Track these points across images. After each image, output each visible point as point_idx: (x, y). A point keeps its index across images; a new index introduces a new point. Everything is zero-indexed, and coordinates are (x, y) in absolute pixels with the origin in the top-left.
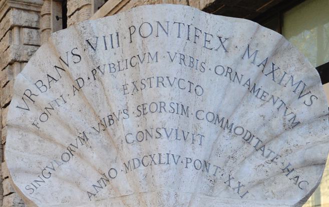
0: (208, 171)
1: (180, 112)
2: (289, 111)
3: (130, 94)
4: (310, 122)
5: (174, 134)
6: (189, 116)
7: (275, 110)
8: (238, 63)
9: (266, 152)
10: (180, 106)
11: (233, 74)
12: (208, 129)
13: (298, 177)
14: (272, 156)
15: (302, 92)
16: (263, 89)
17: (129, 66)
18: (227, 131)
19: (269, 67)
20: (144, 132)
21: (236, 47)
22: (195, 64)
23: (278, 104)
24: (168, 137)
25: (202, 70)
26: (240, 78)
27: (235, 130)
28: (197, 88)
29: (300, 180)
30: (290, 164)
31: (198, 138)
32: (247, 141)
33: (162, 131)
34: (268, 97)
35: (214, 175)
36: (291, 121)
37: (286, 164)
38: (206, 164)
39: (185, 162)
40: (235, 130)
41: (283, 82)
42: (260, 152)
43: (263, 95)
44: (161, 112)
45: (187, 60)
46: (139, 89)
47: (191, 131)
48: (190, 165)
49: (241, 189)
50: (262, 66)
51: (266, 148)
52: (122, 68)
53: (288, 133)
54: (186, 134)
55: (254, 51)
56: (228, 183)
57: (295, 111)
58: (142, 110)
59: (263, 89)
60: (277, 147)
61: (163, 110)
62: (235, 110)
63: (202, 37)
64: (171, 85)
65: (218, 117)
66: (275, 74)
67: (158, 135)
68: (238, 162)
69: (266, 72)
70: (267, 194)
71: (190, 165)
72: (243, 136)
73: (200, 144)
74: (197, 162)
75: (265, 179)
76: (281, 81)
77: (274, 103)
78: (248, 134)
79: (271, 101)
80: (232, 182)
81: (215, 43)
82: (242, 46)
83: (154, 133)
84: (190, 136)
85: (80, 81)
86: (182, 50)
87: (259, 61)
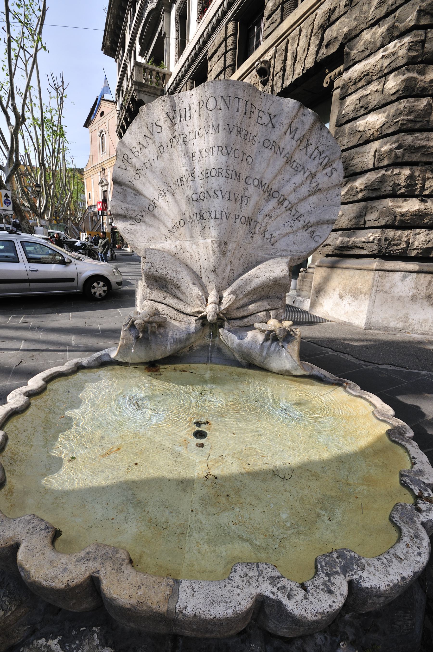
0: (250, 225)
1: (233, 178)
2: (314, 180)
3: (197, 160)
4: (328, 189)
5: (227, 196)
6: (241, 179)
7: (305, 179)
8: (281, 138)
9: (293, 212)
10: (234, 172)
11: (277, 148)
12: (254, 194)
13: (313, 232)
14: (298, 215)
15: (326, 165)
16: (297, 161)
17: (197, 136)
18: (267, 194)
19: (305, 142)
20: (206, 192)
21: (282, 124)
22: (248, 137)
23: (307, 174)
24: (223, 197)
25: (254, 143)
26: (281, 150)
27: (273, 193)
28: (249, 158)
29: (314, 235)
30: (309, 222)
31: (245, 199)
32: (281, 203)
33: (219, 193)
34: (300, 169)
35: (255, 228)
36: (315, 189)
37: (307, 222)
38: (249, 220)
39: (234, 218)
40: (273, 193)
41: (313, 156)
42: (289, 212)
43: (296, 166)
44: (218, 176)
45: (243, 133)
46: (204, 156)
47: (241, 194)
48: (238, 221)
49: (273, 239)
50: (299, 142)
51: (294, 208)
52: (192, 138)
53: (311, 197)
54: (236, 195)
55: (294, 129)
56: (263, 235)
57: (319, 181)
58: (205, 175)
59: (297, 161)
60: (303, 208)
61: (220, 175)
62: (274, 178)
63: (256, 113)
64: (229, 154)
65: (261, 183)
66: (308, 149)
67: (215, 196)
68: (273, 219)
69: (301, 147)
70: (290, 244)
71: (238, 221)
72: (278, 199)
73: (246, 205)
74: (243, 218)
75: (290, 233)
76: (311, 155)
77: (304, 173)
78: (282, 198)
79: (302, 172)
80: (266, 233)
81: (265, 119)
82: (286, 122)
83: (213, 195)
84: (240, 197)
85: (161, 148)
86: (239, 123)
87: (297, 137)
